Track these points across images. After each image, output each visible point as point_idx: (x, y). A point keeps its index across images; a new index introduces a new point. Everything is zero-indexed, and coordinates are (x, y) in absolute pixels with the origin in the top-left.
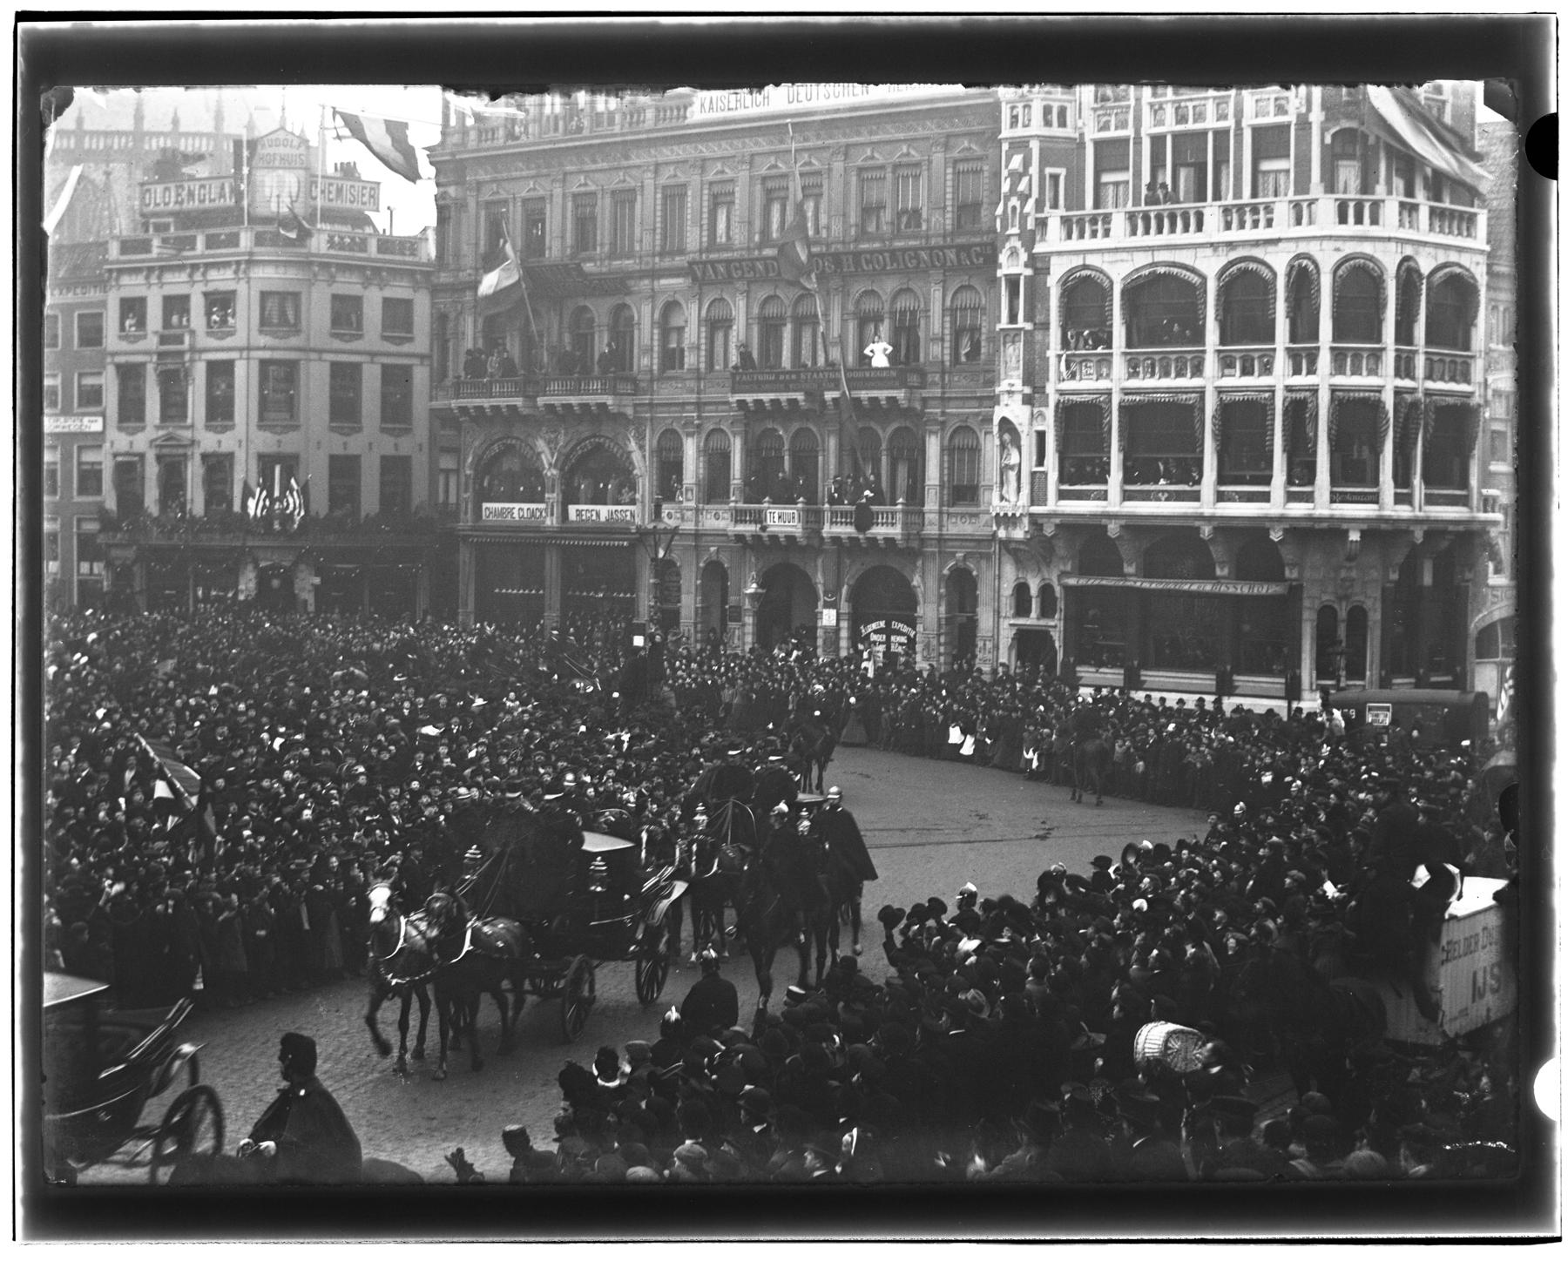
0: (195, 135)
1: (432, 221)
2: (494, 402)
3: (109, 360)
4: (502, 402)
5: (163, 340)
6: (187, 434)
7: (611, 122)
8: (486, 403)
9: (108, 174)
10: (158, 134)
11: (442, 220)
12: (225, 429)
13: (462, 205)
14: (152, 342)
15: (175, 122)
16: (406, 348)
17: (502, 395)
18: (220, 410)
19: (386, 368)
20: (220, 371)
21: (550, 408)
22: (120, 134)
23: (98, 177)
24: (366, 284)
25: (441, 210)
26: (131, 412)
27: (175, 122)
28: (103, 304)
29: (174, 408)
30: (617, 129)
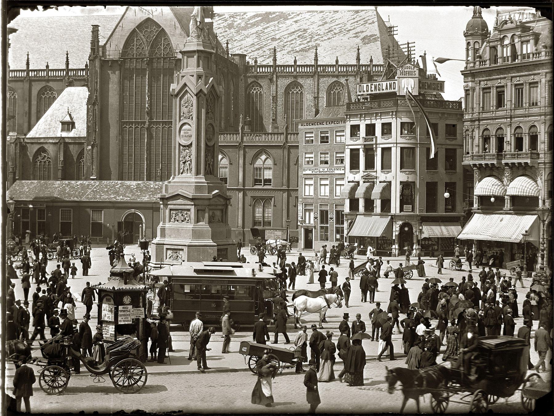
0: (378, 66)
1: (463, 94)
2: (486, 162)
3: (346, 147)
4: (489, 162)
5: (366, 140)
6: (374, 174)
7: (529, 57)
8: (483, 162)
9: (347, 80)
10: (365, 66)
11: (467, 95)
12: (388, 172)
13: (474, 89)
14: (361, 141)
15: (371, 61)
16: (453, 142)
17: (489, 159)
18: (386, 166)
19: (447, 150)
20: (386, 151)
21: (507, 164)
22: (351, 66)
23: (343, 80)
24: (441, 118)
25: (466, 91)
26: (354, 165)
27: (371, 61)
28: (345, 127)
29: (370, 164)
30: (531, 60)
